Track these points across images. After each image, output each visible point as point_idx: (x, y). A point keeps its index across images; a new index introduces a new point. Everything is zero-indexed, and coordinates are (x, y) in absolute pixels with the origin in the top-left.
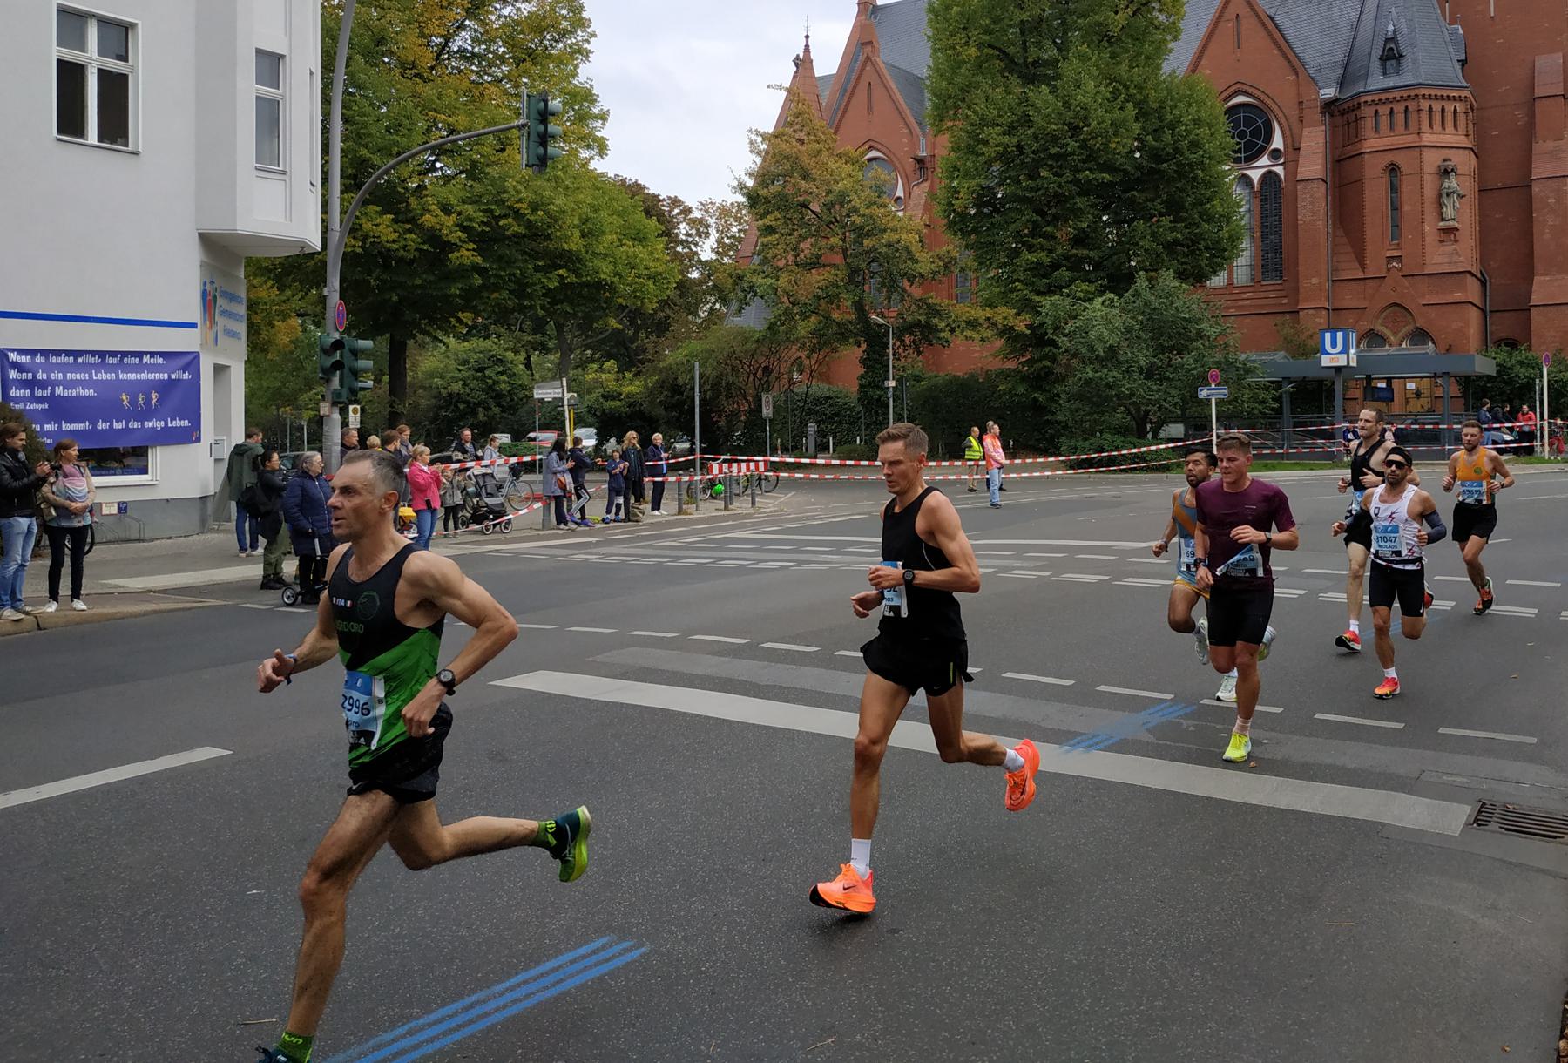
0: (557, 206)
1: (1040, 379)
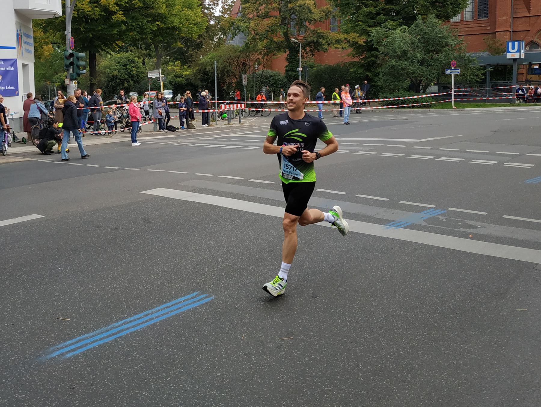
1: (370, 66)
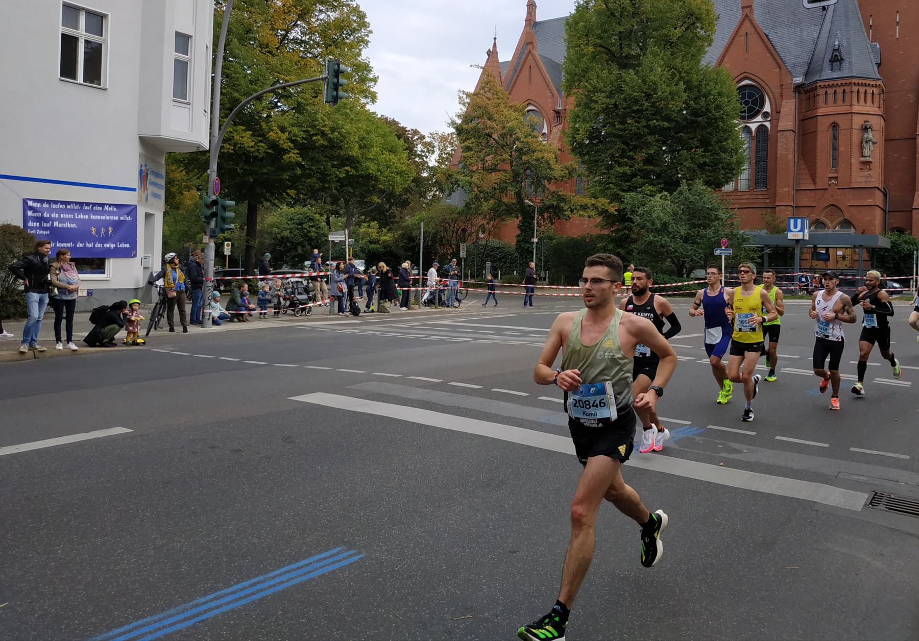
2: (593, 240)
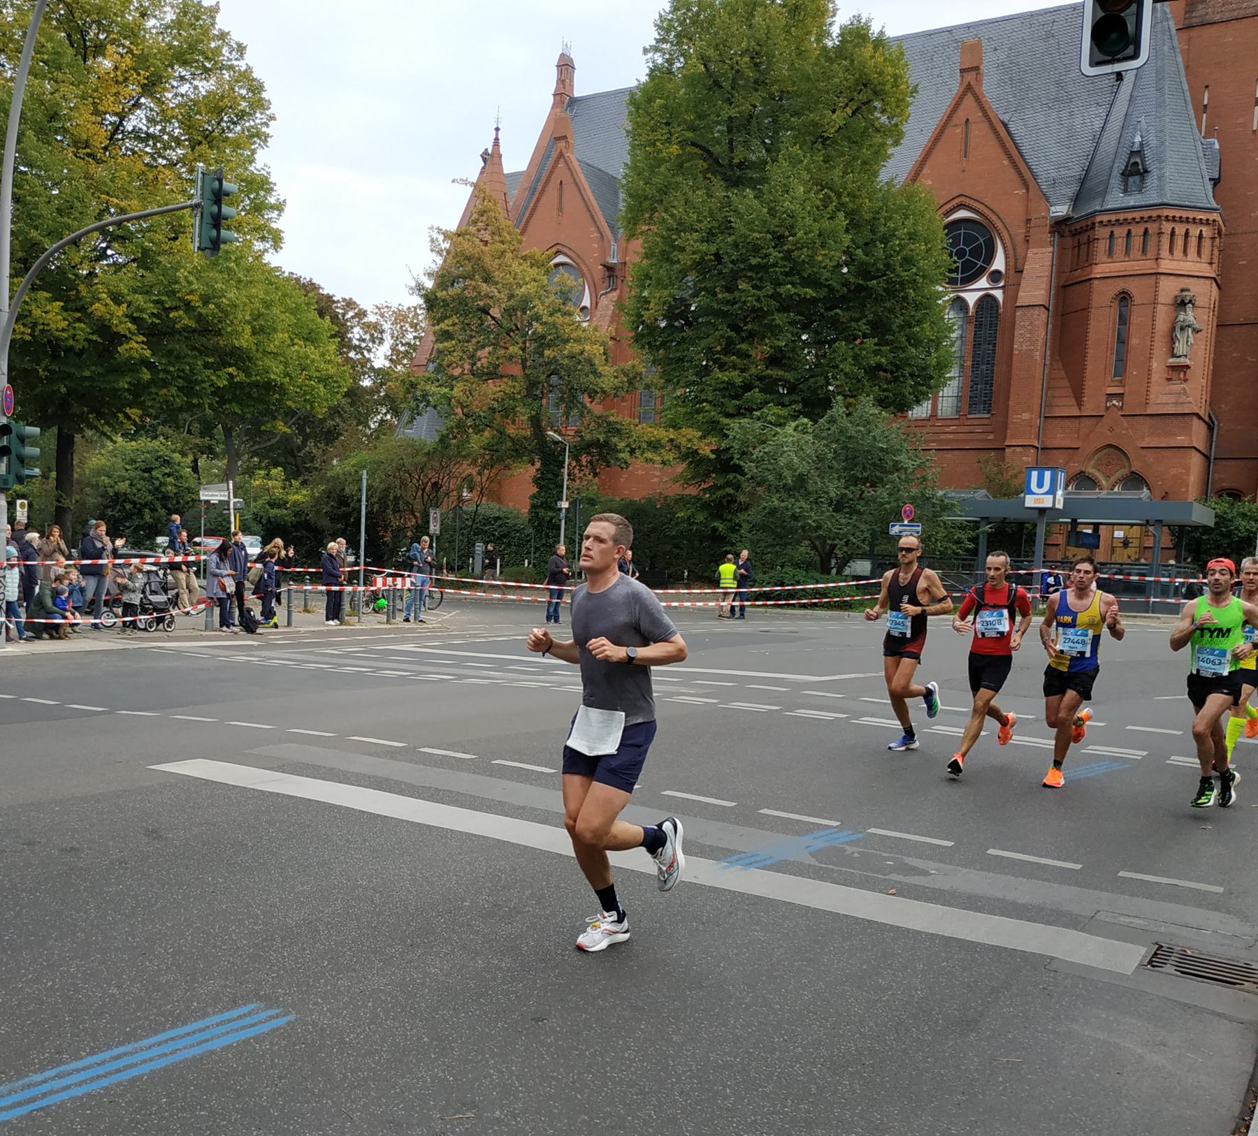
0: (229, 299)
1: (722, 507)
2: (668, 505)
